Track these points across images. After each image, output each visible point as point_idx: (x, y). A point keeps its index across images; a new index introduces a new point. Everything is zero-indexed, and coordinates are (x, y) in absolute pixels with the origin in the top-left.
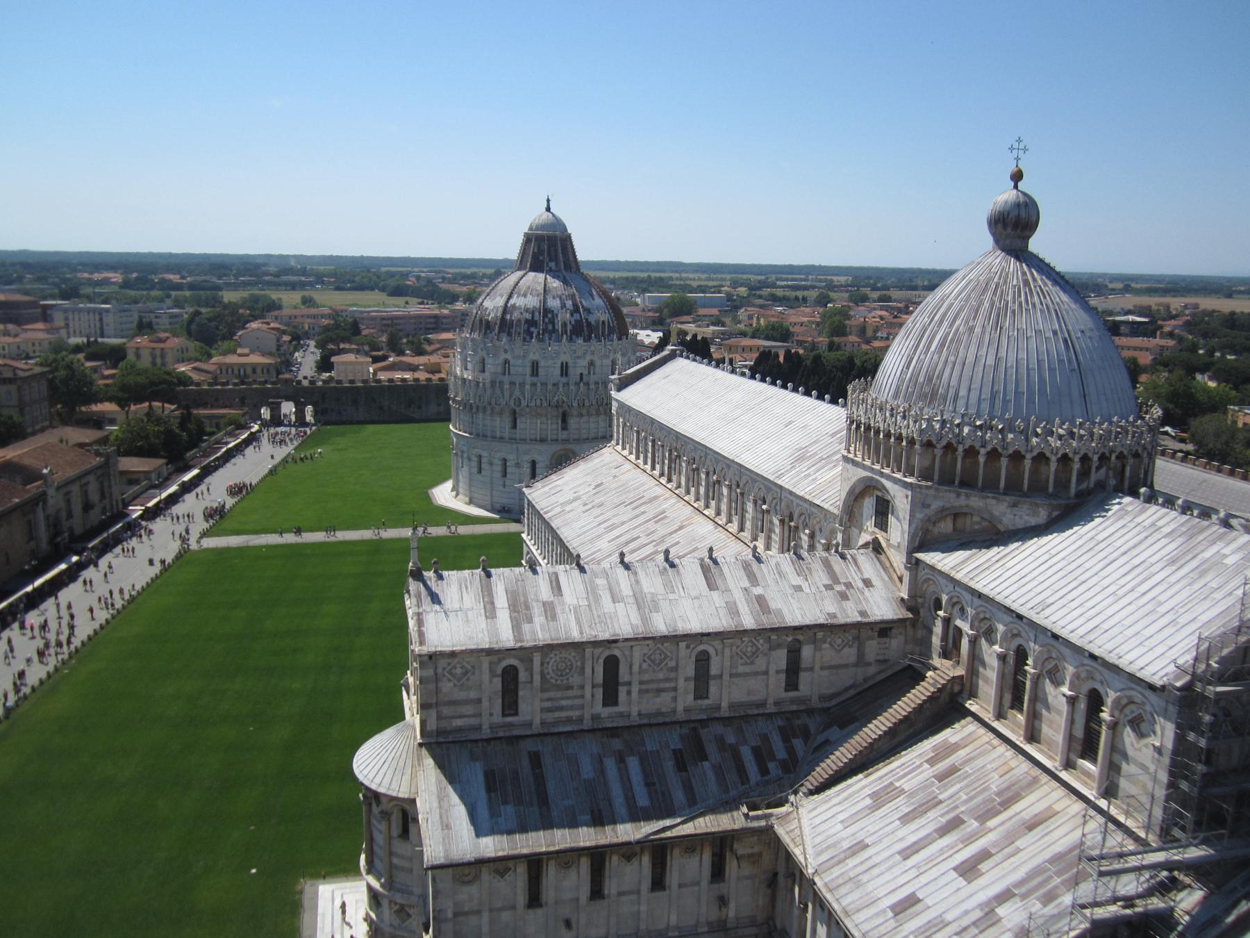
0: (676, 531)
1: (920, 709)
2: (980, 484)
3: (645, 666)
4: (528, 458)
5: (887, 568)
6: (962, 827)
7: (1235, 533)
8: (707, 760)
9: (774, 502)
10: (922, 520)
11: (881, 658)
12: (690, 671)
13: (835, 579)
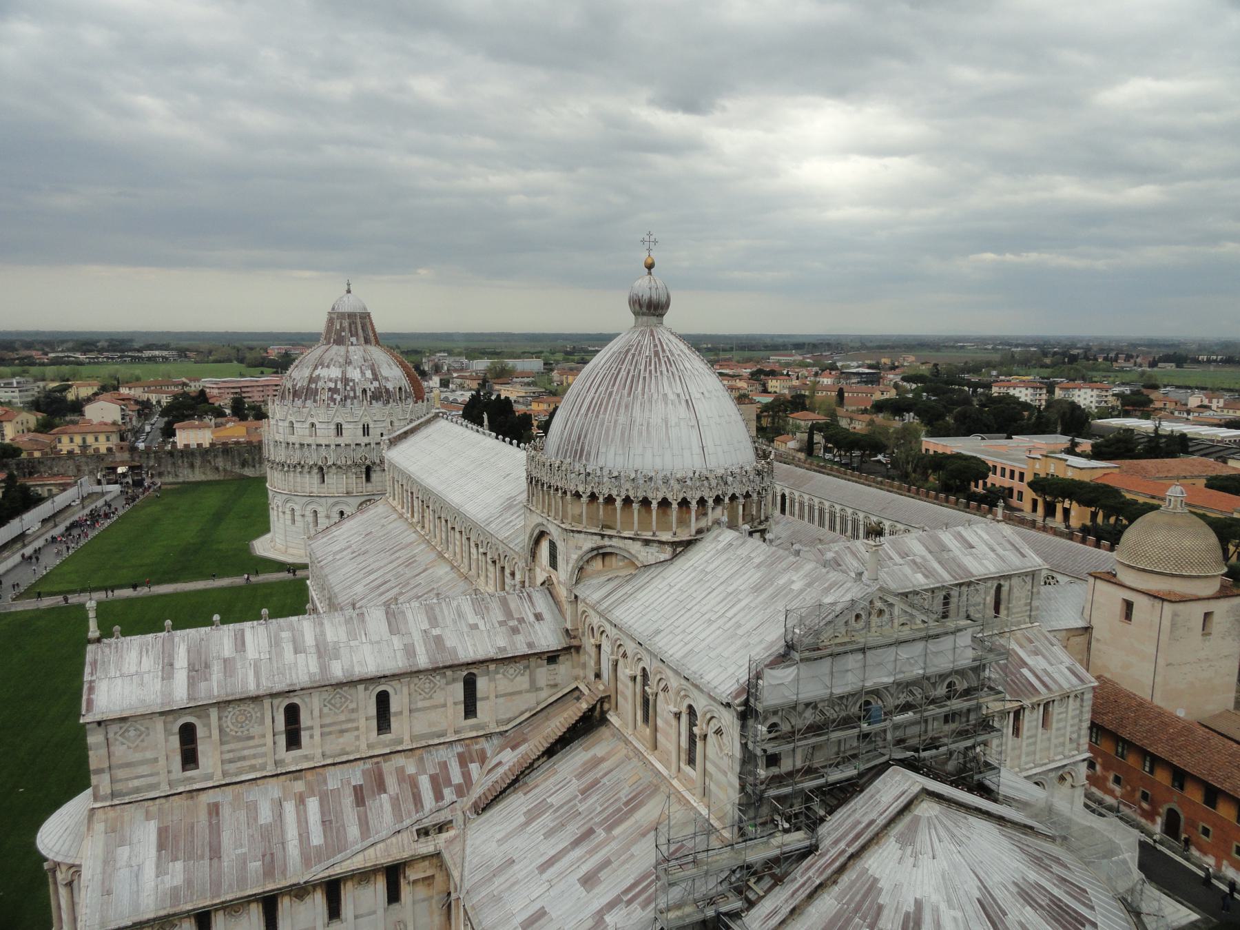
2: (619, 526)
4: (337, 509)
6: (592, 837)
10: (577, 561)
11: (552, 683)
12: (372, 710)
13: (509, 614)
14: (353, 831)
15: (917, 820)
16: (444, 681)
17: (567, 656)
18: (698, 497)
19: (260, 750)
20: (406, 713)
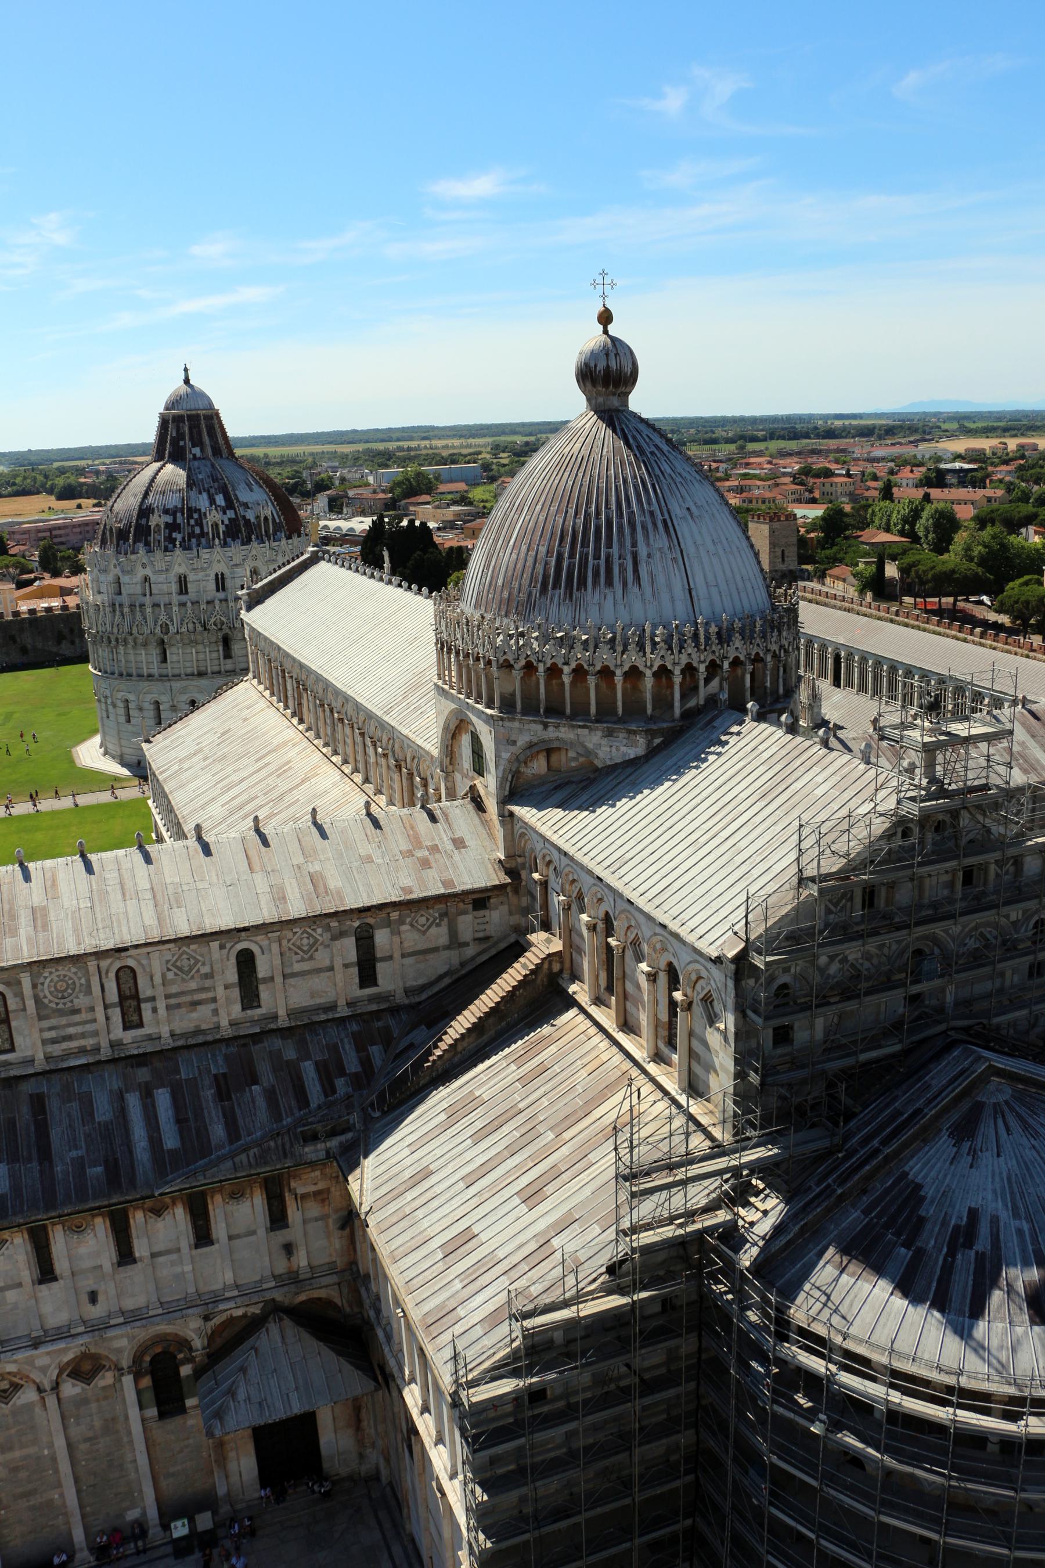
0: (299, 785)
1: (510, 997)
2: (568, 711)
3: (170, 975)
5: (485, 823)
7: (835, 754)
8: (255, 1081)
9: (391, 742)
11: (481, 935)
12: (232, 976)
13: (416, 841)
14: (218, 1131)
15: (978, 1108)
16: (327, 936)
17: (501, 899)
18: (684, 660)
19: (89, 1027)
20: (279, 979)
